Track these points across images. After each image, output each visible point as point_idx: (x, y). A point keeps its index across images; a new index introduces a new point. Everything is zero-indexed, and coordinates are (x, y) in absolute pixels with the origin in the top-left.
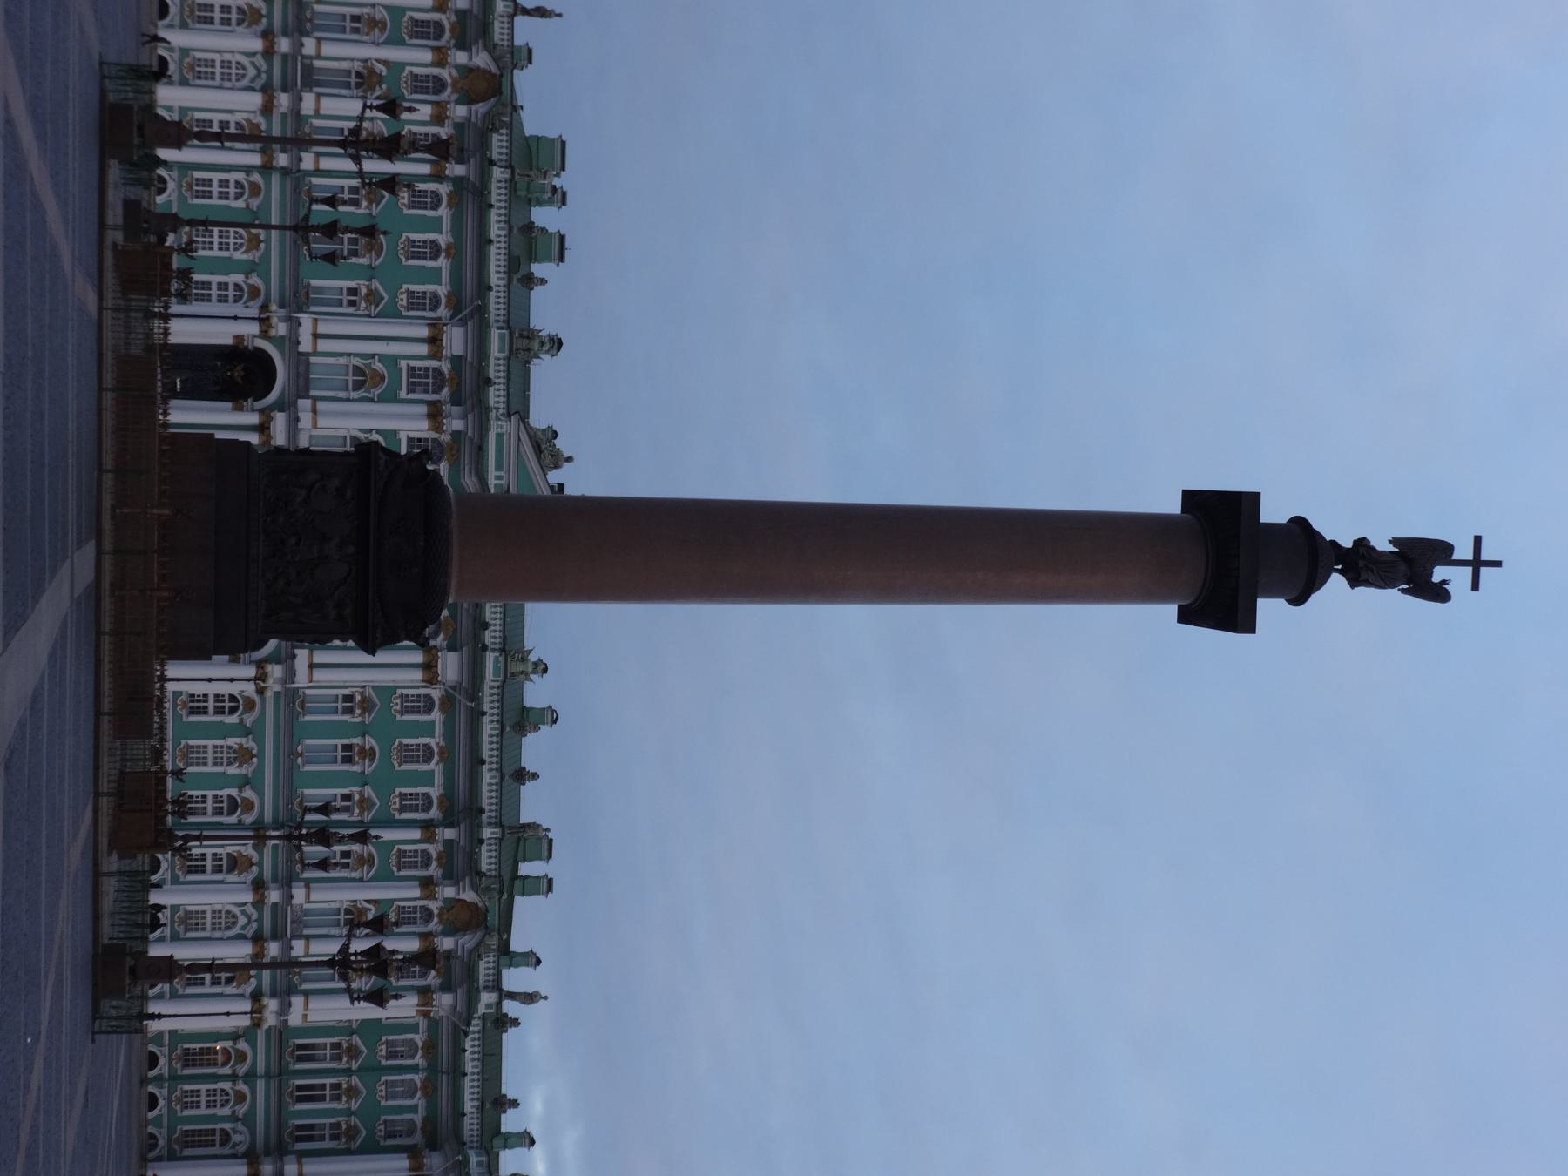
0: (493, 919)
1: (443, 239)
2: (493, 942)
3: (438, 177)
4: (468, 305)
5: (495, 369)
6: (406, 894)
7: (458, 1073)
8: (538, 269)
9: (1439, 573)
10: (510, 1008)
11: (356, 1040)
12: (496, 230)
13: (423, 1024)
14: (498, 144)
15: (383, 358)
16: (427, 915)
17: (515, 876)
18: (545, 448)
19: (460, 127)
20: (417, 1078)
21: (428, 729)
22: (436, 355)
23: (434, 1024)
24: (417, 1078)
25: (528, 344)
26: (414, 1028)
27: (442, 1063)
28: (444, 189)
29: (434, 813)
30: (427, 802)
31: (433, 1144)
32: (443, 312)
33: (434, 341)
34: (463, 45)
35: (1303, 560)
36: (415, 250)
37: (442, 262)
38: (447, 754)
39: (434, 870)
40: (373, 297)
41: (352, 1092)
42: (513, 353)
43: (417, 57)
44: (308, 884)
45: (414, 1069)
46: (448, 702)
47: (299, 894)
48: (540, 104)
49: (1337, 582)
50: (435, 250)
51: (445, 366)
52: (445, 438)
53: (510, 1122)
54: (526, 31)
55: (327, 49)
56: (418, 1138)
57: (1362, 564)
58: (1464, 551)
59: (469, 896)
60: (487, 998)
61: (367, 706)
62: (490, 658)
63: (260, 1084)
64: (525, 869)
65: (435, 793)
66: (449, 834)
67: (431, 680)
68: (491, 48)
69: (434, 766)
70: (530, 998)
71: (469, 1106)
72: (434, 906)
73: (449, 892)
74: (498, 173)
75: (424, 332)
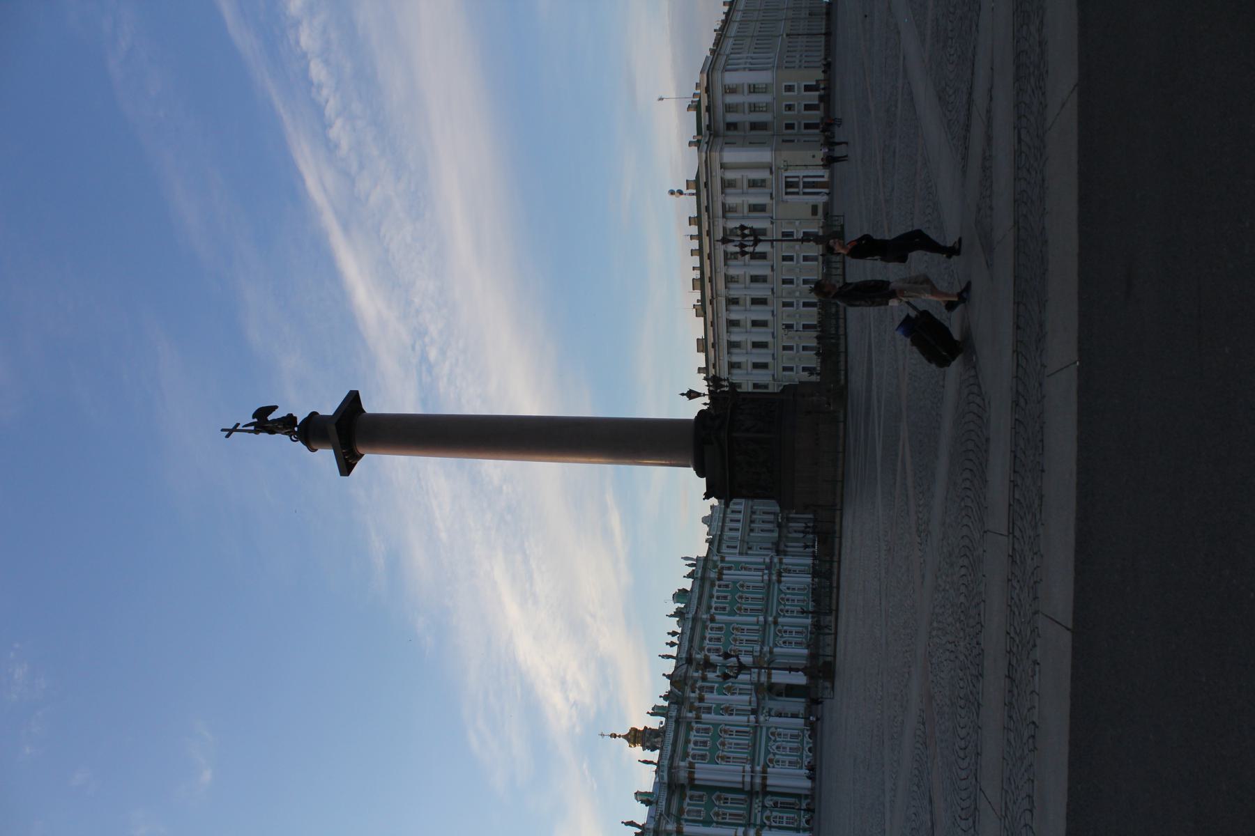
20: (686, 816)
24: (686, 816)
31: (683, 786)
41: (717, 814)
45: (687, 820)
56: (689, 793)
63: (758, 822)
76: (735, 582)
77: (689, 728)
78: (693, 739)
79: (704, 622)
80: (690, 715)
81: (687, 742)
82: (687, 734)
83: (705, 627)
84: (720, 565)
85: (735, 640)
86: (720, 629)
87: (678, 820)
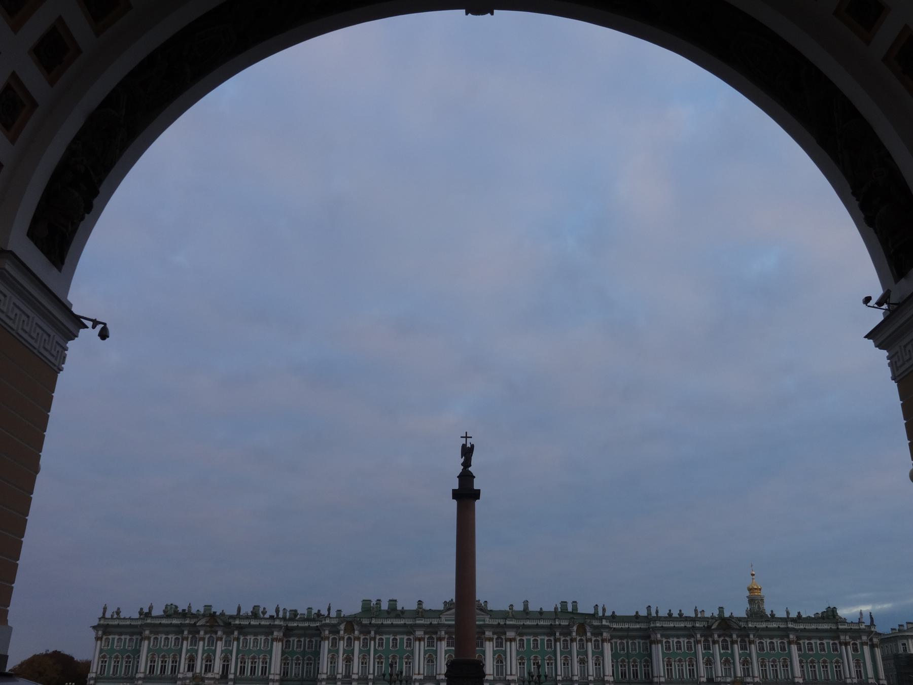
0: (582, 621)
1: (392, 637)
2: (588, 621)
3: (374, 639)
4: (409, 630)
5: (427, 622)
6: (575, 646)
7: (628, 629)
8: (399, 608)
9: (469, 445)
10: (608, 613)
11: (619, 660)
12: (389, 622)
13: (613, 641)
14: (365, 621)
15: (425, 654)
16: (581, 640)
17: (572, 613)
18: (448, 606)
19: (361, 633)
20: (630, 642)
21: (528, 640)
22: (424, 639)
23: (612, 637)
25: (420, 612)
26: (616, 643)
27: (625, 634)
28: (378, 637)
29: (552, 638)
30: (549, 640)
31: (649, 637)
32: (411, 637)
33: (420, 640)
34: (338, 632)
35: (466, 477)
36: (395, 645)
37: (398, 637)
38: (535, 635)
39: (568, 638)
40: (408, 657)
41: (635, 661)
42: (423, 617)
43: (342, 645)
44: (573, 675)
45: (627, 643)
46: (521, 634)
47: (576, 678)
48: (352, 608)
49: (470, 469)
50: (395, 639)
51: (427, 636)
52: (447, 636)
53: (643, 613)
54: (333, 614)
55: (340, 671)
56: (648, 641)
57: (467, 464)
58: (463, 441)
59: (575, 628)
60: (604, 622)
61: (522, 658)
62: (508, 623)
64: (570, 609)
65: (546, 638)
66: (558, 634)
67: (514, 640)
68: (339, 624)
69: (539, 638)
70: (604, 610)
71: (638, 626)
72: (578, 638)
73: (574, 634)
74: (373, 621)
75: (417, 643)
76: (841, 656)
77: (689, 636)
78: (681, 640)
79: (788, 637)
80: (699, 636)
81: (678, 637)
82: (683, 636)
83: (782, 637)
84: (858, 642)
85: (774, 661)
86: (783, 649)
87: (612, 637)
